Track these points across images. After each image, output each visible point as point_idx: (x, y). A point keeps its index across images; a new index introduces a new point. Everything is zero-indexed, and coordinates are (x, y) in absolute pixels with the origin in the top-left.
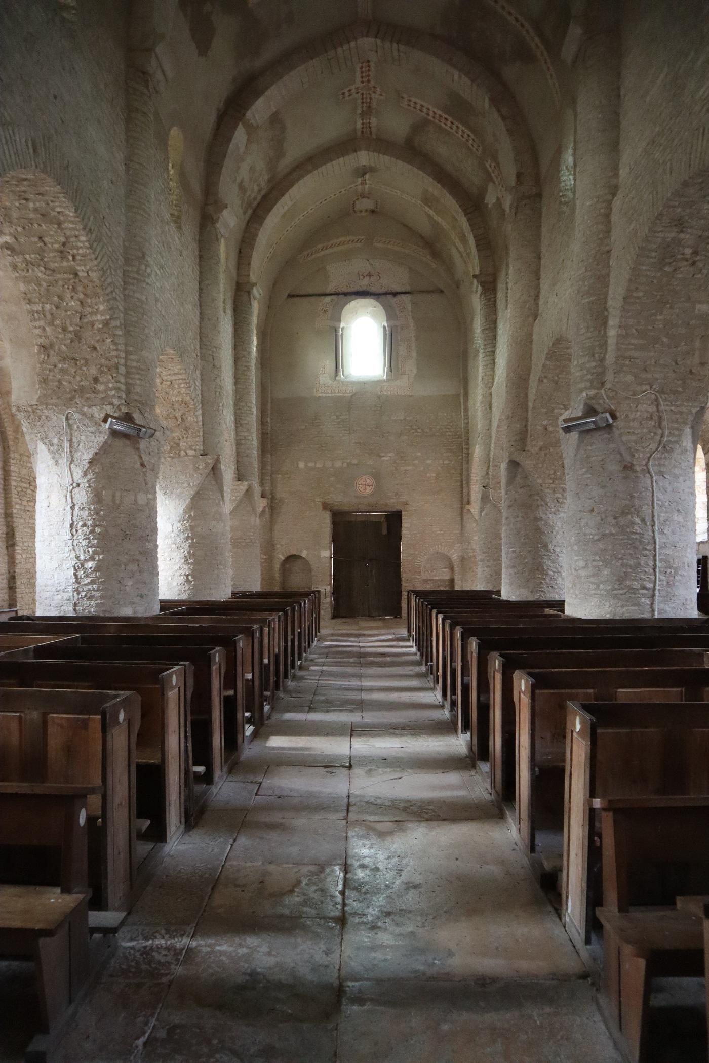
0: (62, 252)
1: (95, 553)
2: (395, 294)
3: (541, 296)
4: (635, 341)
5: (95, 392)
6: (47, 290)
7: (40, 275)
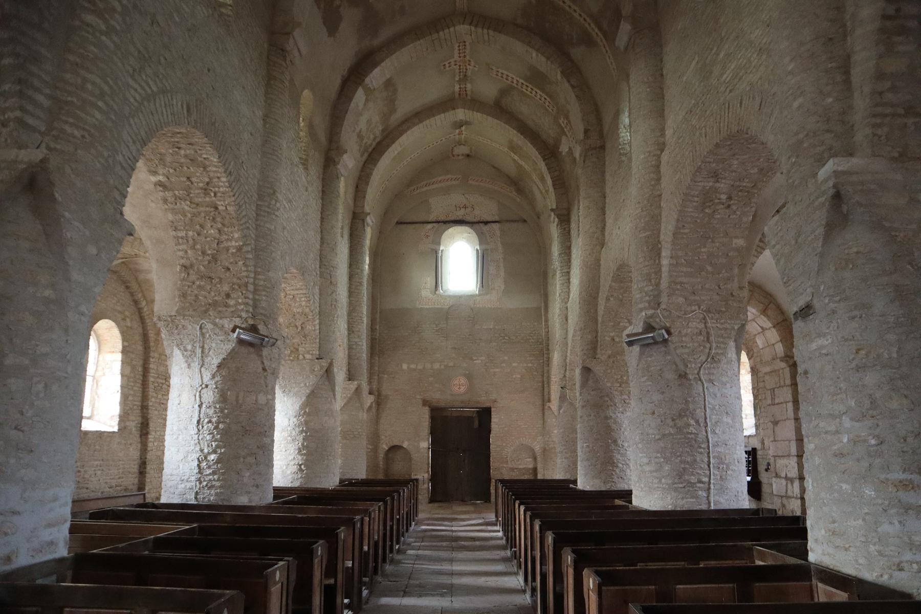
0: (205, 190)
1: (217, 447)
2: (486, 223)
3: (607, 228)
4: (685, 270)
5: (227, 306)
6: (191, 220)
7: (186, 207)
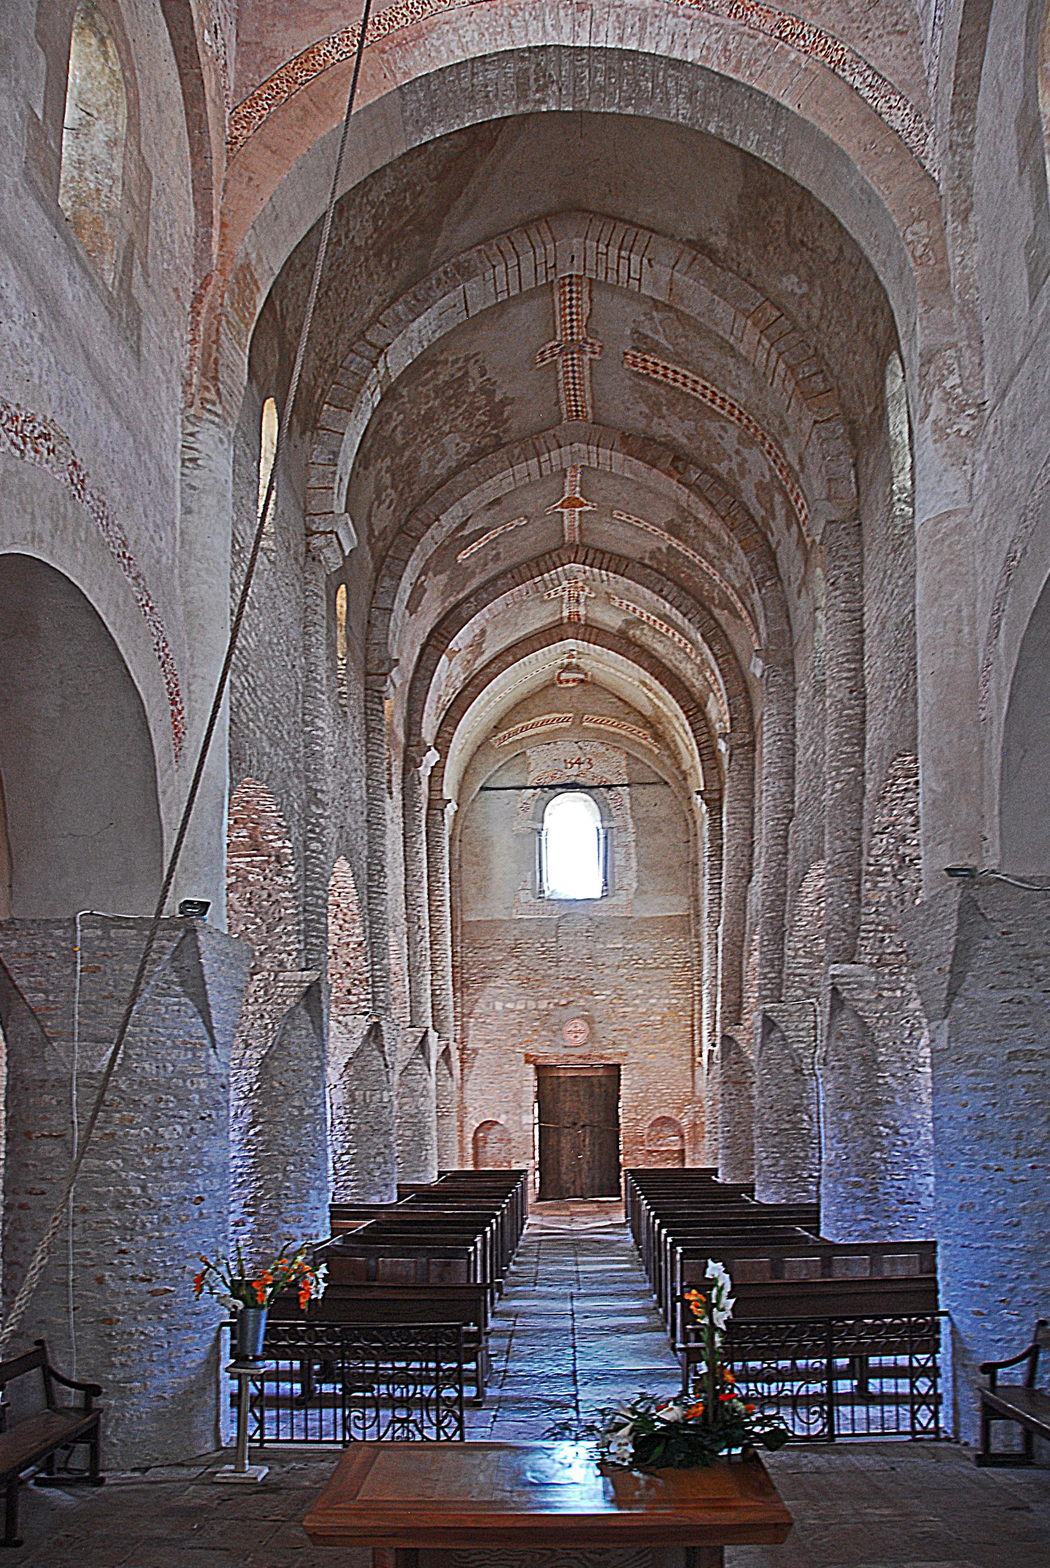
4: (803, 961)
